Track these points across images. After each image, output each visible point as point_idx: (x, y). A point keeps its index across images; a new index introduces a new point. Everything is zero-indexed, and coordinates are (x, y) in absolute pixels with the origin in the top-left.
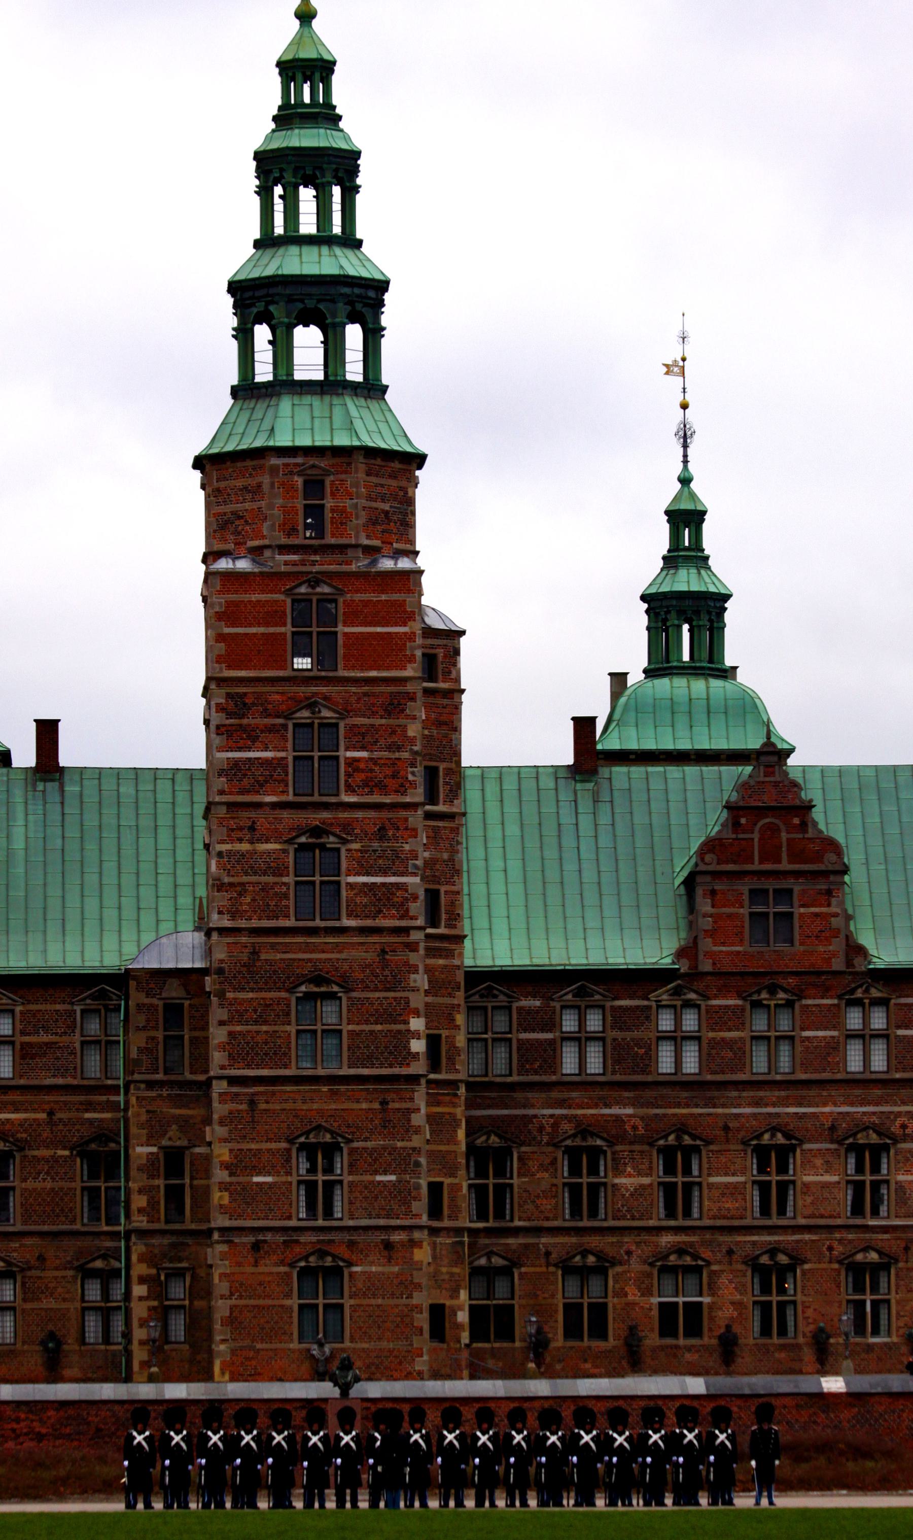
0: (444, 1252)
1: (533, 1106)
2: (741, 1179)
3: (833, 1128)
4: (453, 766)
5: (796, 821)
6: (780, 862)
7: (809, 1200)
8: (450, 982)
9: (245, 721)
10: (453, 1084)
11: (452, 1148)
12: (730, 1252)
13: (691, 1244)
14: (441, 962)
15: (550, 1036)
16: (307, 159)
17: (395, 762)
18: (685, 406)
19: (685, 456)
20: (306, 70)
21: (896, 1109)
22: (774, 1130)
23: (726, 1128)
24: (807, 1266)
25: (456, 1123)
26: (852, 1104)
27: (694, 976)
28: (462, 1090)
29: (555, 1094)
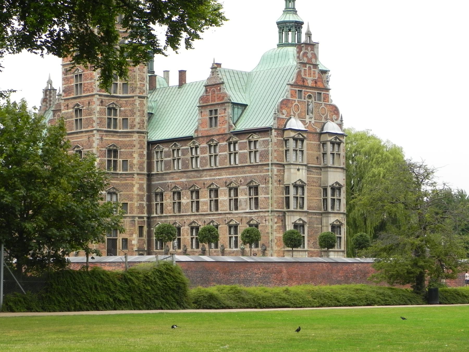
0: (128, 223)
1: (166, 180)
2: (207, 199)
3: (226, 183)
4: (133, 82)
5: (219, 88)
6: (215, 101)
7: (221, 205)
8: (131, 145)
9: (67, 76)
10: (133, 174)
11: (131, 193)
12: (205, 222)
13: (197, 220)
14: (128, 139)
15: (169, 159)
17: (91, 83)
21: (239, 176)
22: (212, 184)
23: (204, 184)
24: (220, 226)
25: (133, 186)
26: (230, 175)
27: (197, 138)
28: (136, 176)
29: (171, 176)
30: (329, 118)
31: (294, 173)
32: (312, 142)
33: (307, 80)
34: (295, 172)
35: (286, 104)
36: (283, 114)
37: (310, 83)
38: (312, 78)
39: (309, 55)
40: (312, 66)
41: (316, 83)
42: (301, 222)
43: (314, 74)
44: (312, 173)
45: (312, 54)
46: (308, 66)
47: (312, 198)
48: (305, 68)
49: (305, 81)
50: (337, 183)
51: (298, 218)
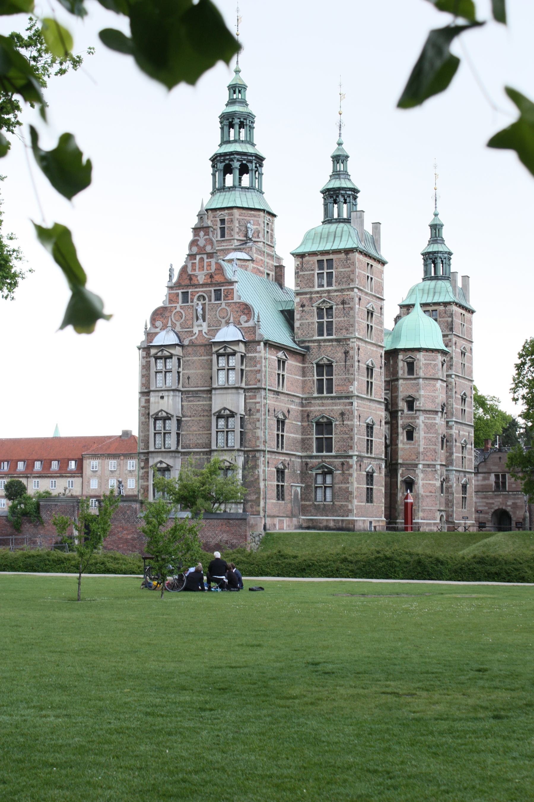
19: (340, 134)
30: (232, 320)
31: (155, 403)
32: (203, 358)
33: (197, 276)
34: (157, 400)
35: (161, 314)
36: (156, 327)
37: (201, 279)
38: (205, 271)
39: (201, 243)
40: (205, 256)
41: (211, 277)
42: (164, 465)
43: (209, 265)
44: (202, 399)
45: (206, 240)
46: (198, 257)
47: (201, 432)
48: (194, 261)
49: (194, 278)
50: (225, 409)
51: (159, 459)
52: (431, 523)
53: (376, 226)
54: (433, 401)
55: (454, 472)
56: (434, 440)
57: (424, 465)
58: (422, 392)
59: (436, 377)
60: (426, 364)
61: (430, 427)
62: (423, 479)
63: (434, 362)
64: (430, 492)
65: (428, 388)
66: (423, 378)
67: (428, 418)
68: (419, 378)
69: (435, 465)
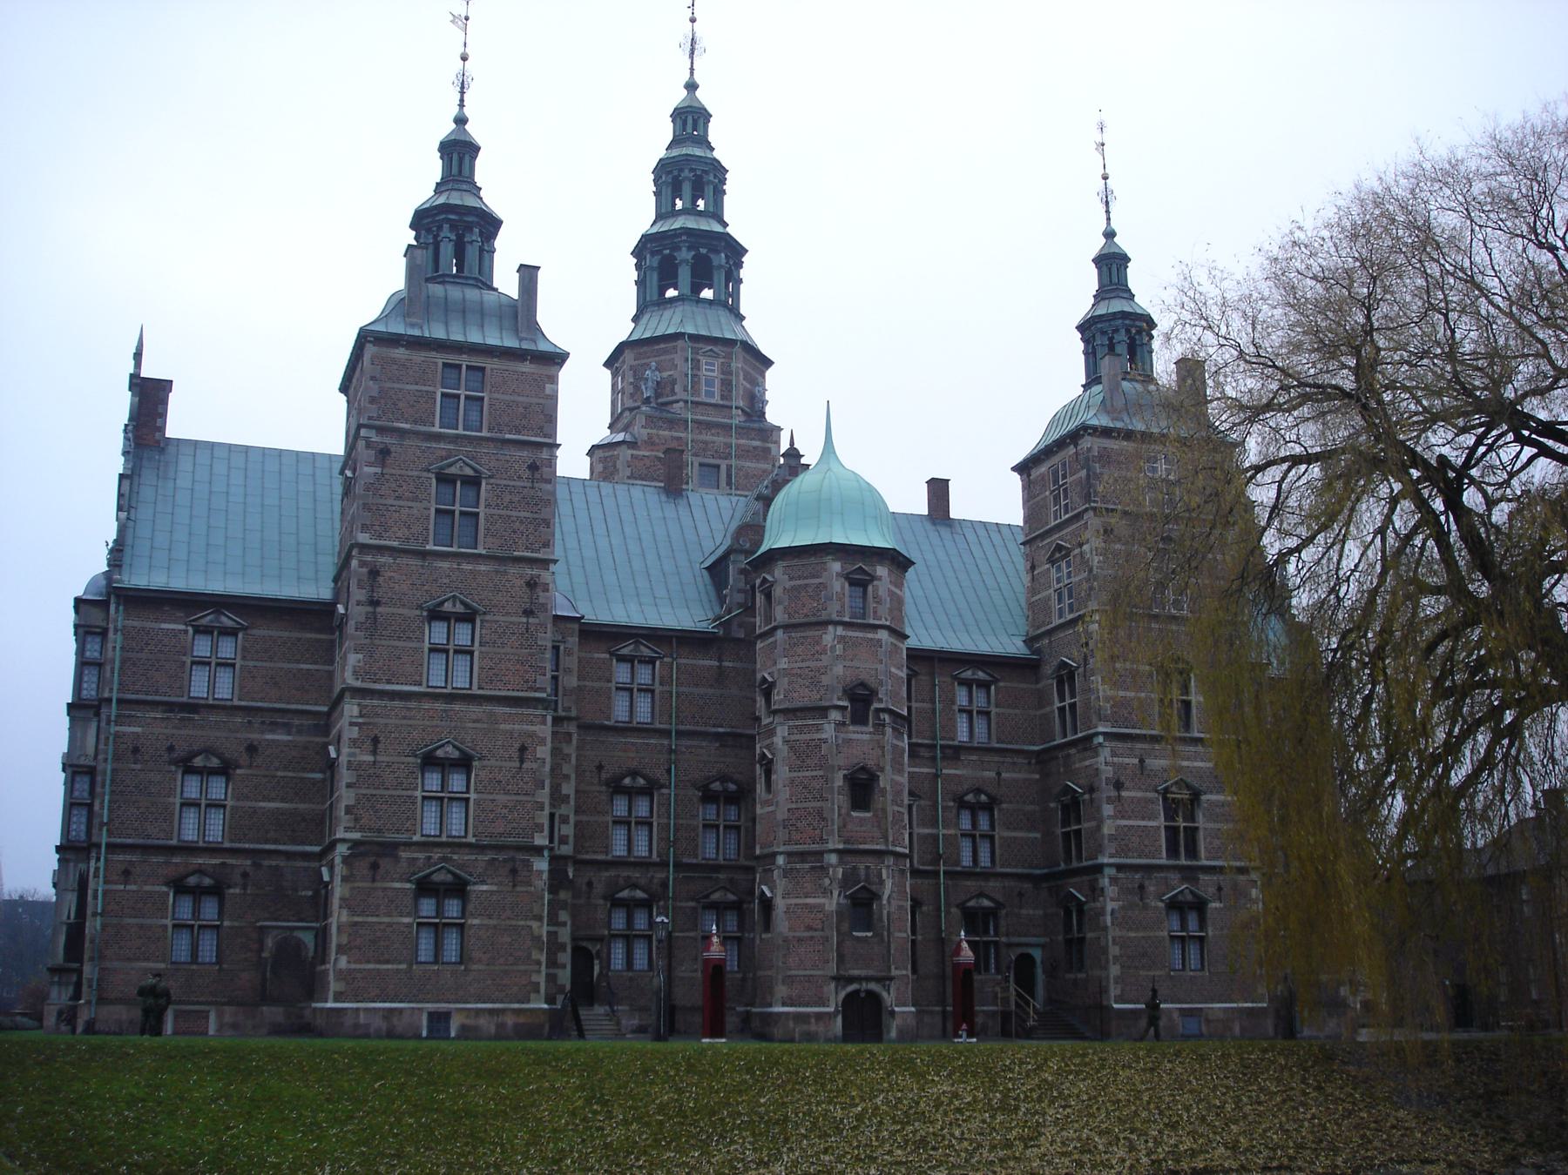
16: (689, 173)
18: (464, 58)
19: (462, 100)
20: (691, 120)
52: (808, 1015)
53: (528, 274)
54: (815, 684)
55: (1113, 871)
56: (816, 784)
57: (789, 854)
58: (783, 664)
59: (824, 617)
60: (793, 588)
61: (802, 754)
62: (786, 895)
63: (817, 581)
64: (809, 928)
65: (799, 650)
66: (787, 627)
67: (800, 729)
68: (775, 629)
69: (821, 853)
